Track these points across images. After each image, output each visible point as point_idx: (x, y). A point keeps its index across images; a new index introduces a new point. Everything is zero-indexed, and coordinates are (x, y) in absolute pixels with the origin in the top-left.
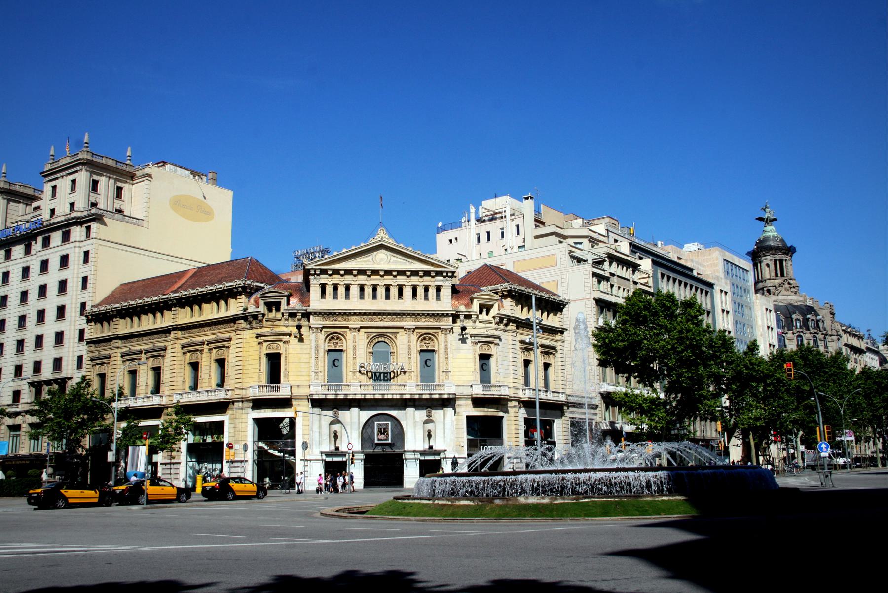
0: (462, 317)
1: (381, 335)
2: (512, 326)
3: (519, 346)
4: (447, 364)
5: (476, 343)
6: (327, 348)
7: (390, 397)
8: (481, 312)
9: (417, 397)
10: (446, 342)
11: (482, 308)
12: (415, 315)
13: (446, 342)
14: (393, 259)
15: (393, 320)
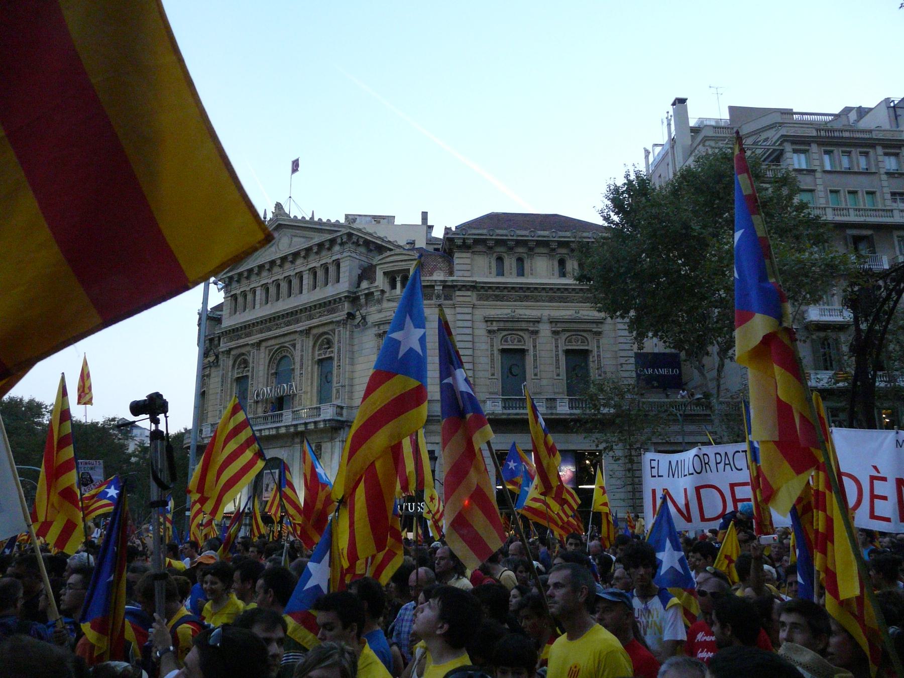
0: (363, 300)
1: (282, 347)
2: (460, 297)
3: (481, 330)
4: (338, 375)
5: (380, 336)
6: (236, 376)
7: (266, 433)
8: (393, 287)
9: (292, 430)
10: (339, 342)
11: (391, 277)
12: (308, 310)
13: (339, 342)
14: (295, 239)
15: (288, 324)
